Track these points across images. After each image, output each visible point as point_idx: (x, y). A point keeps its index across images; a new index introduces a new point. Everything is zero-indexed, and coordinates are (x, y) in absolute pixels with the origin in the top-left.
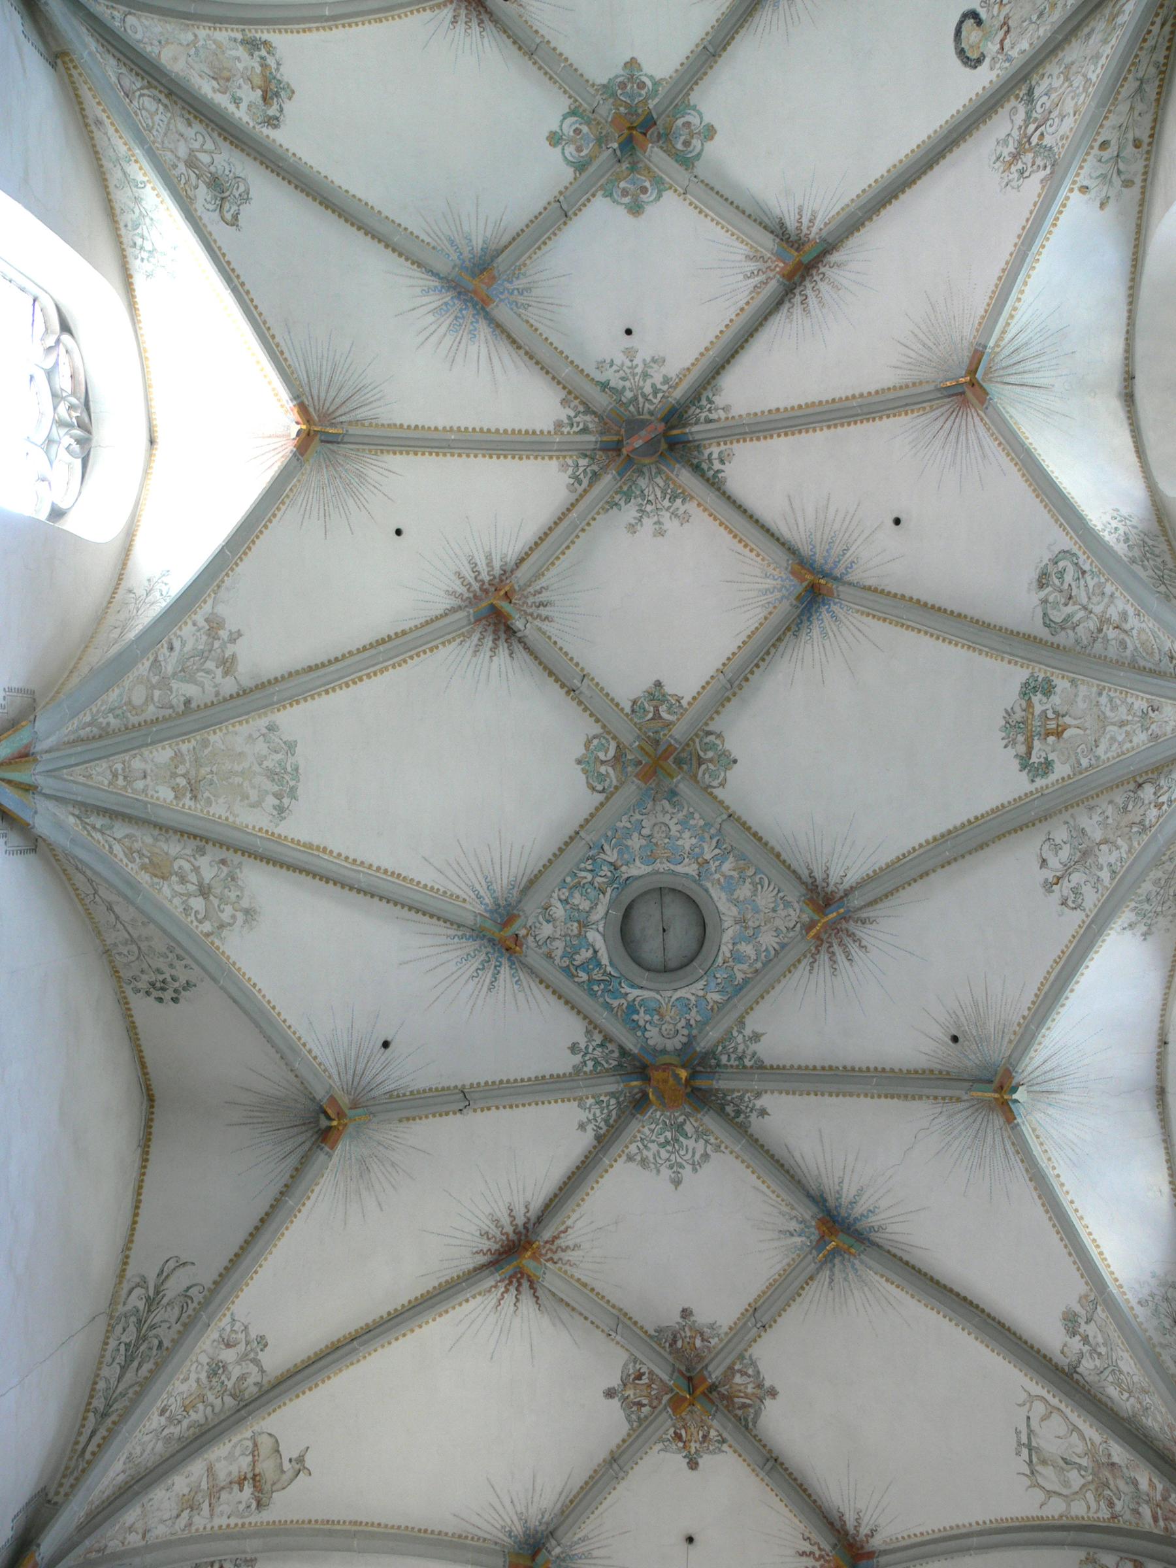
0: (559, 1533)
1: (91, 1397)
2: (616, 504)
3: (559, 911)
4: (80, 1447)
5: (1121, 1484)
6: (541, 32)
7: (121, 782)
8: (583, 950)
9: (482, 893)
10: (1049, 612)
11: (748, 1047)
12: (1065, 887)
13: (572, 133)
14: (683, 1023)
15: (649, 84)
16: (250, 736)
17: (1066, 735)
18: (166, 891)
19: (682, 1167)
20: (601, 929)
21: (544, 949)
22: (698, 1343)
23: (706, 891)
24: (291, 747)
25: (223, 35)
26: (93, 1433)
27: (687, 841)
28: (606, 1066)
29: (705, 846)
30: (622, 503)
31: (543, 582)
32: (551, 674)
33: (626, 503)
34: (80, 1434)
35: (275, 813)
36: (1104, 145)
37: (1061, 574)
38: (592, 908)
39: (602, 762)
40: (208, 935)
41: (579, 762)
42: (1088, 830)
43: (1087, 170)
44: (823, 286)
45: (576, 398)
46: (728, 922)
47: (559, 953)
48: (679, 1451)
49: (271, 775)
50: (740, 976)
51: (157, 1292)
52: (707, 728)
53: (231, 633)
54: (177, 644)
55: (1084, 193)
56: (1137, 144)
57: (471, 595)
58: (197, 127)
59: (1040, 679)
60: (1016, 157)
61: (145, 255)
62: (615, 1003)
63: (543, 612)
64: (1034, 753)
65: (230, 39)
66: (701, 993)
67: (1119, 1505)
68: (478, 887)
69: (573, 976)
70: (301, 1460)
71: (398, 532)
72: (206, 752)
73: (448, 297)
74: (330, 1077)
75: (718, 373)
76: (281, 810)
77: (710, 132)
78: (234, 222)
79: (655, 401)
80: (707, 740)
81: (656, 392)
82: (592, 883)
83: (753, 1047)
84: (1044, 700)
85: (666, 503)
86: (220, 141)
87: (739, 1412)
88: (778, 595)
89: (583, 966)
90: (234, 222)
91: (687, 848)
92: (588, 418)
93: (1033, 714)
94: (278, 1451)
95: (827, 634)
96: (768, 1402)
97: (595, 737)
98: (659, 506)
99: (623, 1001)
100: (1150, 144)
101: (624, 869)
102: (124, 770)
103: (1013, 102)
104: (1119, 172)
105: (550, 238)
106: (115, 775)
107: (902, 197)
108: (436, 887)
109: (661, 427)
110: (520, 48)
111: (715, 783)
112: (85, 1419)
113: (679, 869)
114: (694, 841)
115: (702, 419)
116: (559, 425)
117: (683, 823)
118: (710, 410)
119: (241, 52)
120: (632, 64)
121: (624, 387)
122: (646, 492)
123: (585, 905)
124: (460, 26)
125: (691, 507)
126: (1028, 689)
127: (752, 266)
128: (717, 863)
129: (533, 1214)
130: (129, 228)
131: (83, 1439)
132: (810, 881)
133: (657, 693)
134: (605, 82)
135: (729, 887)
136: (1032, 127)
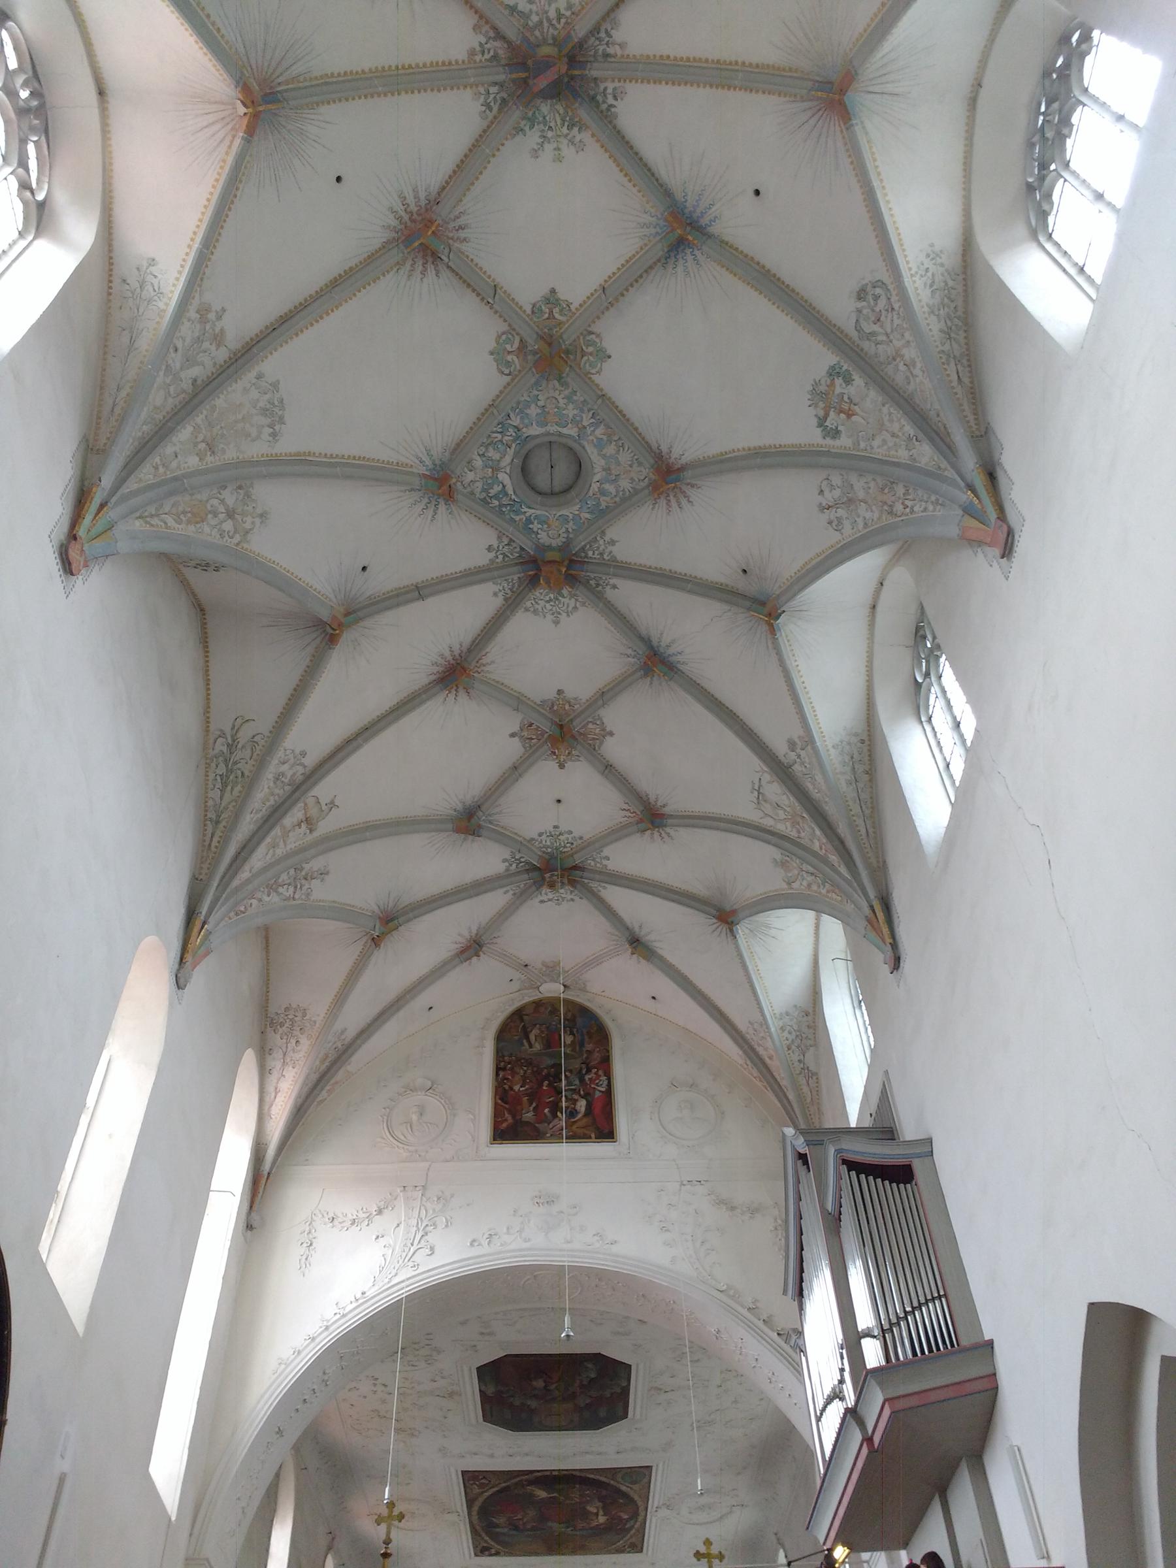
0: (484, 808)
1: (206, 811)
2: (522, 130)
3: (478, 463)
4: (207, 843)
5: (806, 827)
7: (161, 470)
8: (496, 486)
9: (424, 459)
10: (861, 320)
11: (607, 547)
12: (832, 514)
14: (564, 530)
16: (245, 389)
17: (854, 418)
18: (207, 529)
19: (559, 614)
20: (508, 471)
21: (469, 489)
22: (567, 707)
23: (584, 447)
24: (275, 386)
27: (571, 411)
28: (511, 557)
29: (584, 416)
30: (527, 128)
31: (460, 209)
32: (469, 285)
33: (530, 129)
34: (204, 835)
35: (271, 439)
37: (876, 298)
38: (501, 458)
39: (509, 353)
40: (238, 544)
41: (492, 353)
42: (856, 488)
46: (598, 469)
47: (479, 490)
48: (554, 760)
49: (265, 412)
50: (603, 505)
51: (234, 741)
52: (590, 329)
53: (217, 312)
54: (179, 345)
57: (403, 226)
59: (844, 369)
62: (517, 518)
63: (462, 234)
64: (829, 419)
66: (577, 513)
67: (803, 834)
68: (421, 455)
69: (489, 503)
70: (332, 802)
71: (339, 179)
72: (215, 415)
74: (330, 600)
76: (274, 435)
79: (558, 26)
80: (588, 338)
81: (560, 16)
82: (501, 441)
83: (610, 548)
84: (844, 385)
85: (565, 130)
87: (591, 742)
88: (653, 231)
89: (496, 497)
91: (571, 416)
92: (498, 44)
93: (833, 392)
94: (319, 802)
95: (688, 272)
96: (608, 738)
97: (503, 333)
98: (559, 133)
99: (522, 516)
101: (524, 430)
102: (161, 460)
106: (156, 468)
108: (391, 460)
111: (593, 371)
112: (205, 825)
113: (565, 431)
114: (575, 412)
115: (600, 52)
116: (472, 53)
117: (569, 398)
118: (607, 44)
121: (531, 11)
122: (547, 118)
123: (497, 456)
125: (586, 136)
126: (833, 372)
128: (592, 429)
129: (464, 649)
131: (208, 839)
132: (657, 451)
133: (552, 298)
135: (600, 445)
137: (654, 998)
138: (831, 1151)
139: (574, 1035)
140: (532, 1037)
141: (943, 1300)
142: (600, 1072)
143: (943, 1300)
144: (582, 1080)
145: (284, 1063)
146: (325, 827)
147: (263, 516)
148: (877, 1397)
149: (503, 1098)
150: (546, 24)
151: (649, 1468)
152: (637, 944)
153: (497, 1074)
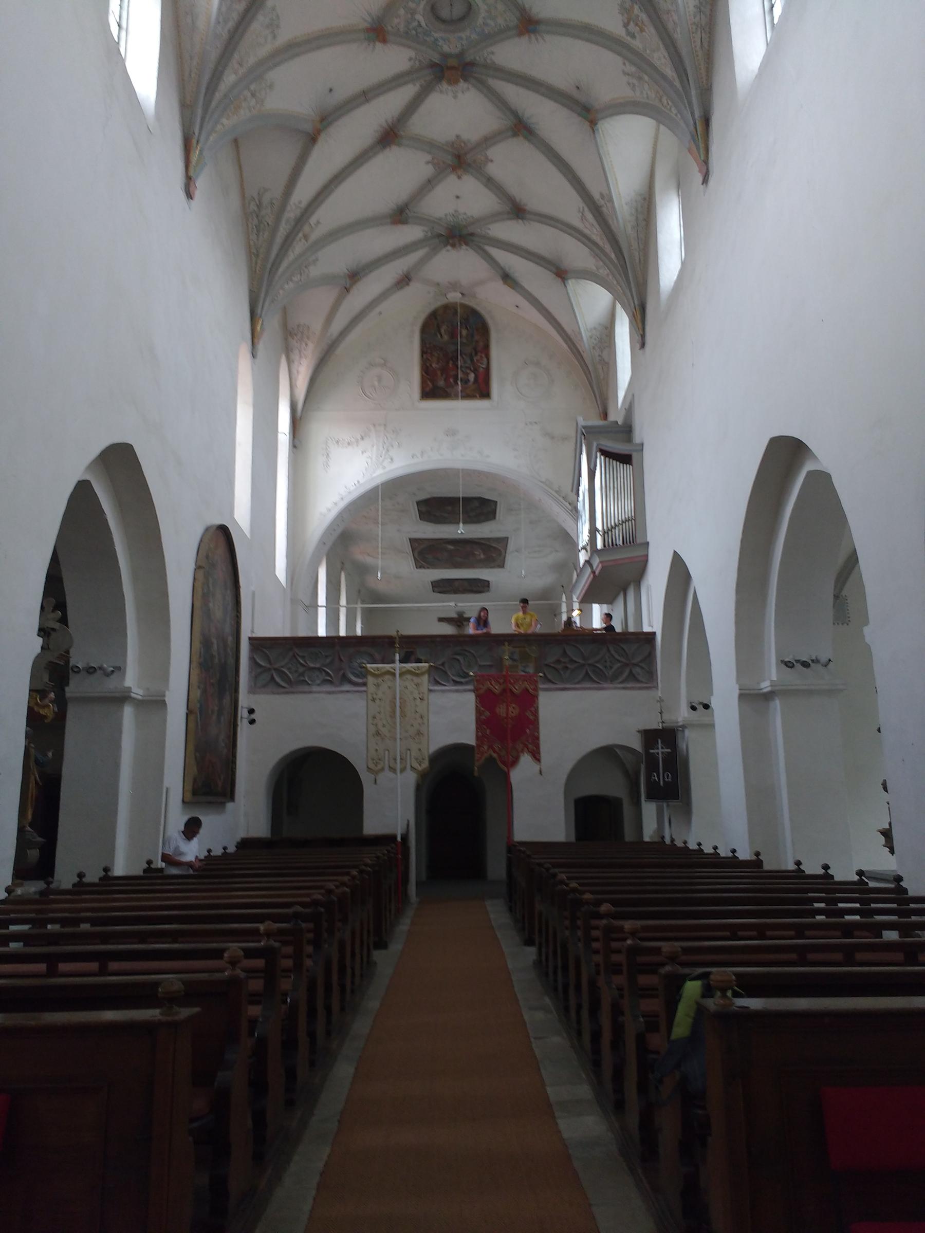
26: (256, 263)
62: (428, 39)
112: (251, 257)
131: (253, 265)
137: (517, 306)
138: (595, 444)
139: (467, 329)
140: (443, 331)
141: (633, 521)
142: (483, 356)
143: (633, 521)
144: (472, 360)
145: (301, 357)
146: (313, 237)
147: (271, 87)
148: (596, 562)
149: (426, 371)
151: (507, 538)
152: (507, 278)
153: (422, 356)
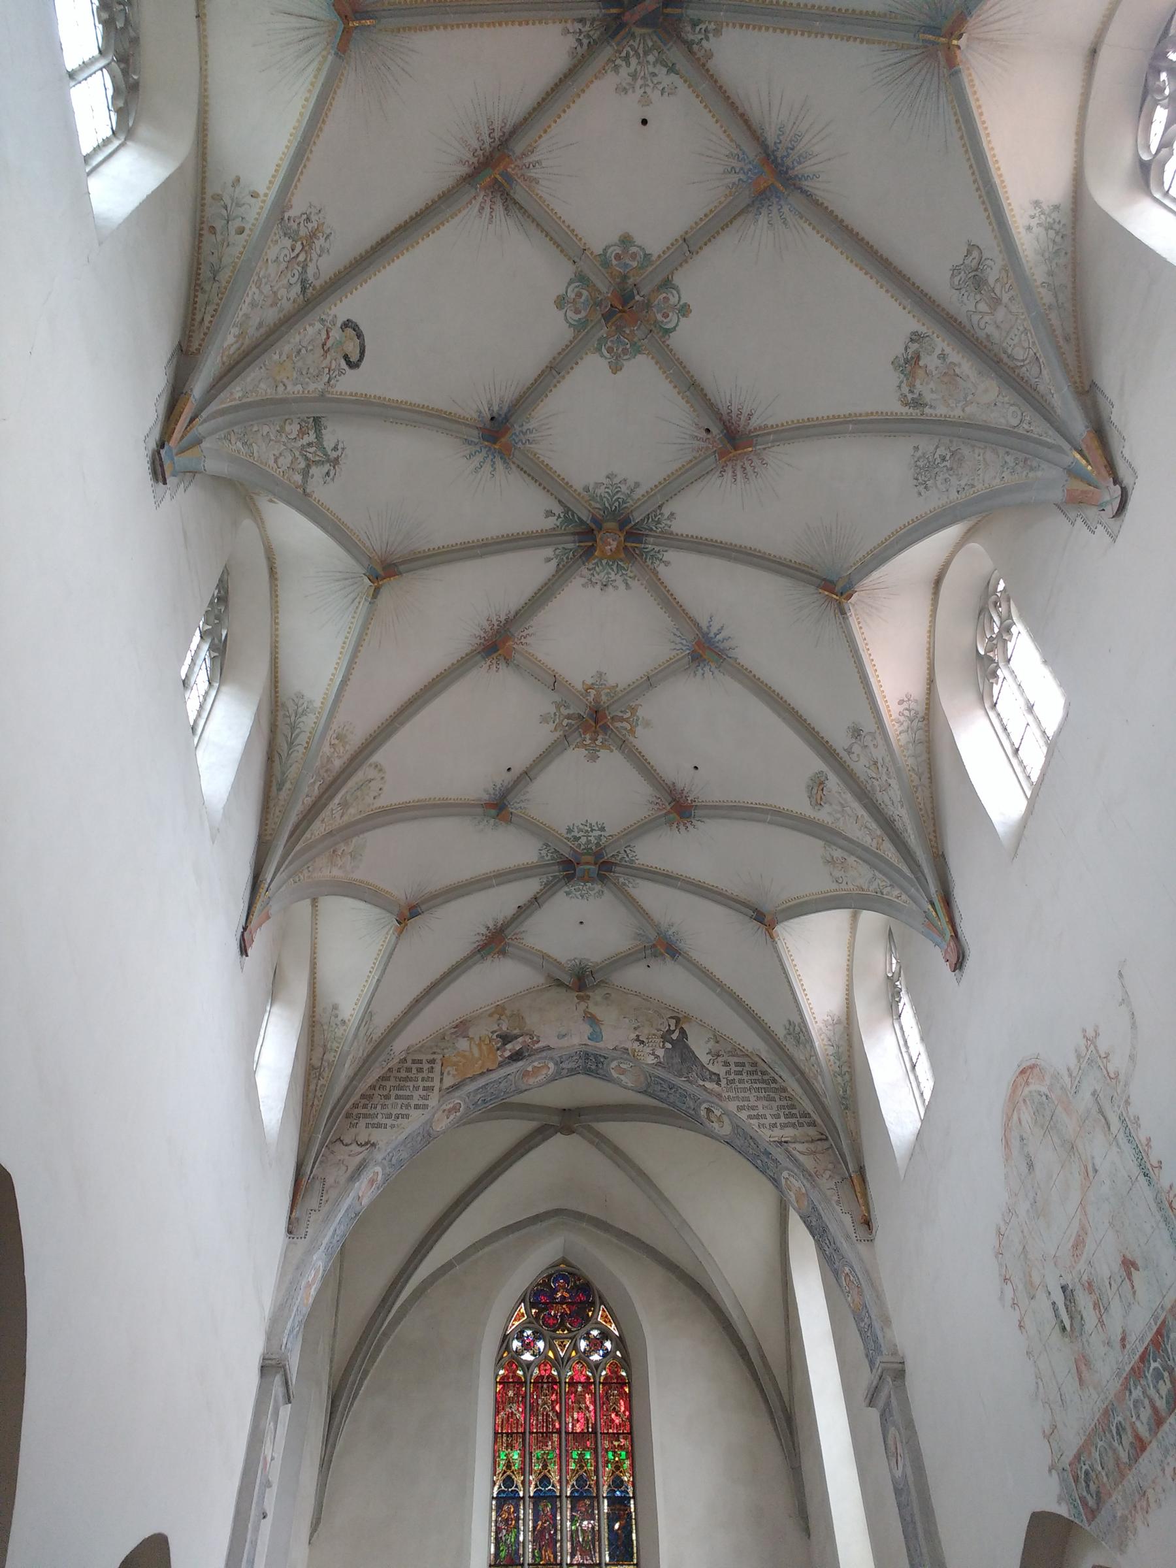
6: (683, 402)
13: (671, 314)
15: (604, 351)
25: (941, 411)
36: (241, 231)
43: (255, 213)
44: (475, 144)
45: (698, 59)
55: (254, 192)
56: (212, 229)
58: (981, 334)
60: (313, 235)
61: (1056, 227)
65: (935, 408)
73: (798, 169)
75: (570, 70)
77: (561, 302)
78: (972, 247)
79: (629, 49)
81: (627, 59)
86: (965, 321)
90: (972, 247)
92: (690, 37)
100: (202, 229)
103: (317, 283)
104: (226, 207)
105: (701, 220)
107: (407, 217)
109: (627, 17)
110: (702, 390)
115: (588, 24)
116: (718, 32)
119: (928, 397)
120: (616, 368)
121: (654, 66)
124: (746, 412)
127: (533, 173)
130: (1064, 252)
134: (639, 357)
136: (301, 258)
150: (641, 51)
